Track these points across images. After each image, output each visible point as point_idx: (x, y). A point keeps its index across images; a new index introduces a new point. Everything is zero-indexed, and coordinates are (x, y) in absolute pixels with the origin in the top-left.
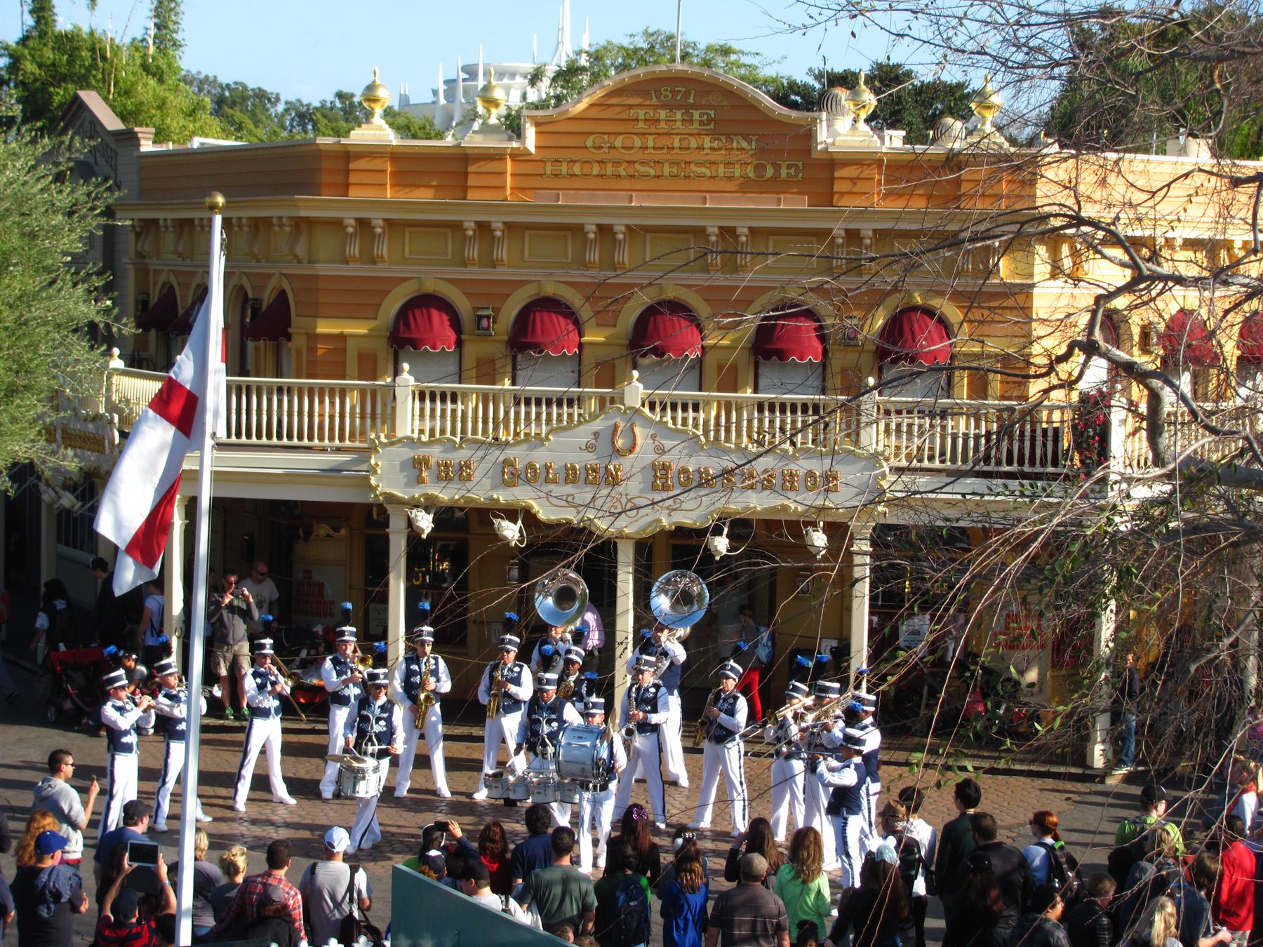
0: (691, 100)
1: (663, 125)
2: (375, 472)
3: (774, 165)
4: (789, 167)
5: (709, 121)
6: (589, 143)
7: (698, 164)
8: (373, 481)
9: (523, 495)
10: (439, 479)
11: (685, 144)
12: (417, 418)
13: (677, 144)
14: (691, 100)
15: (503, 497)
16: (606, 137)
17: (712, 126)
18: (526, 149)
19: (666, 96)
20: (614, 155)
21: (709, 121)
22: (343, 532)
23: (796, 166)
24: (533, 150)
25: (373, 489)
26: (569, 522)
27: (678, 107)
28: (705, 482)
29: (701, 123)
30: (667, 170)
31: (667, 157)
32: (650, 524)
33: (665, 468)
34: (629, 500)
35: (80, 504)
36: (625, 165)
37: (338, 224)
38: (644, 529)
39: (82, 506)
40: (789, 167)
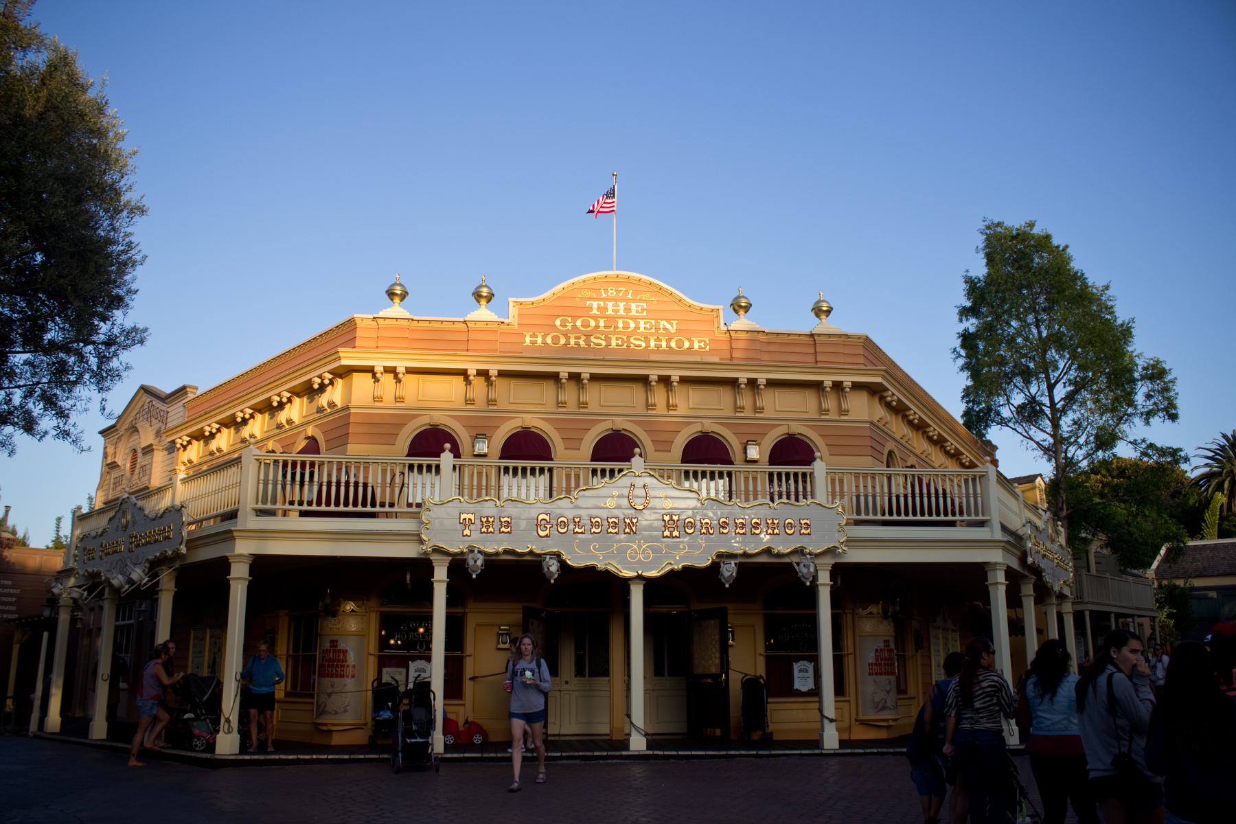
0: (630, 296)
3: (689, 340)
4: (700, 342)
5: (643, 310)
6: (558, 322)
13: (620, 325)
14: (630, 296)
16: (570, 319)
17: (645, 314)
19: (612, 293)
21: (643, 310)
23: (705, 341)
27: (622, 300)
29: (637, 312)
35: (147, 579)
36: (584, 338)
37: (370, 370)
39: (148, 581)
40: (700, 342)
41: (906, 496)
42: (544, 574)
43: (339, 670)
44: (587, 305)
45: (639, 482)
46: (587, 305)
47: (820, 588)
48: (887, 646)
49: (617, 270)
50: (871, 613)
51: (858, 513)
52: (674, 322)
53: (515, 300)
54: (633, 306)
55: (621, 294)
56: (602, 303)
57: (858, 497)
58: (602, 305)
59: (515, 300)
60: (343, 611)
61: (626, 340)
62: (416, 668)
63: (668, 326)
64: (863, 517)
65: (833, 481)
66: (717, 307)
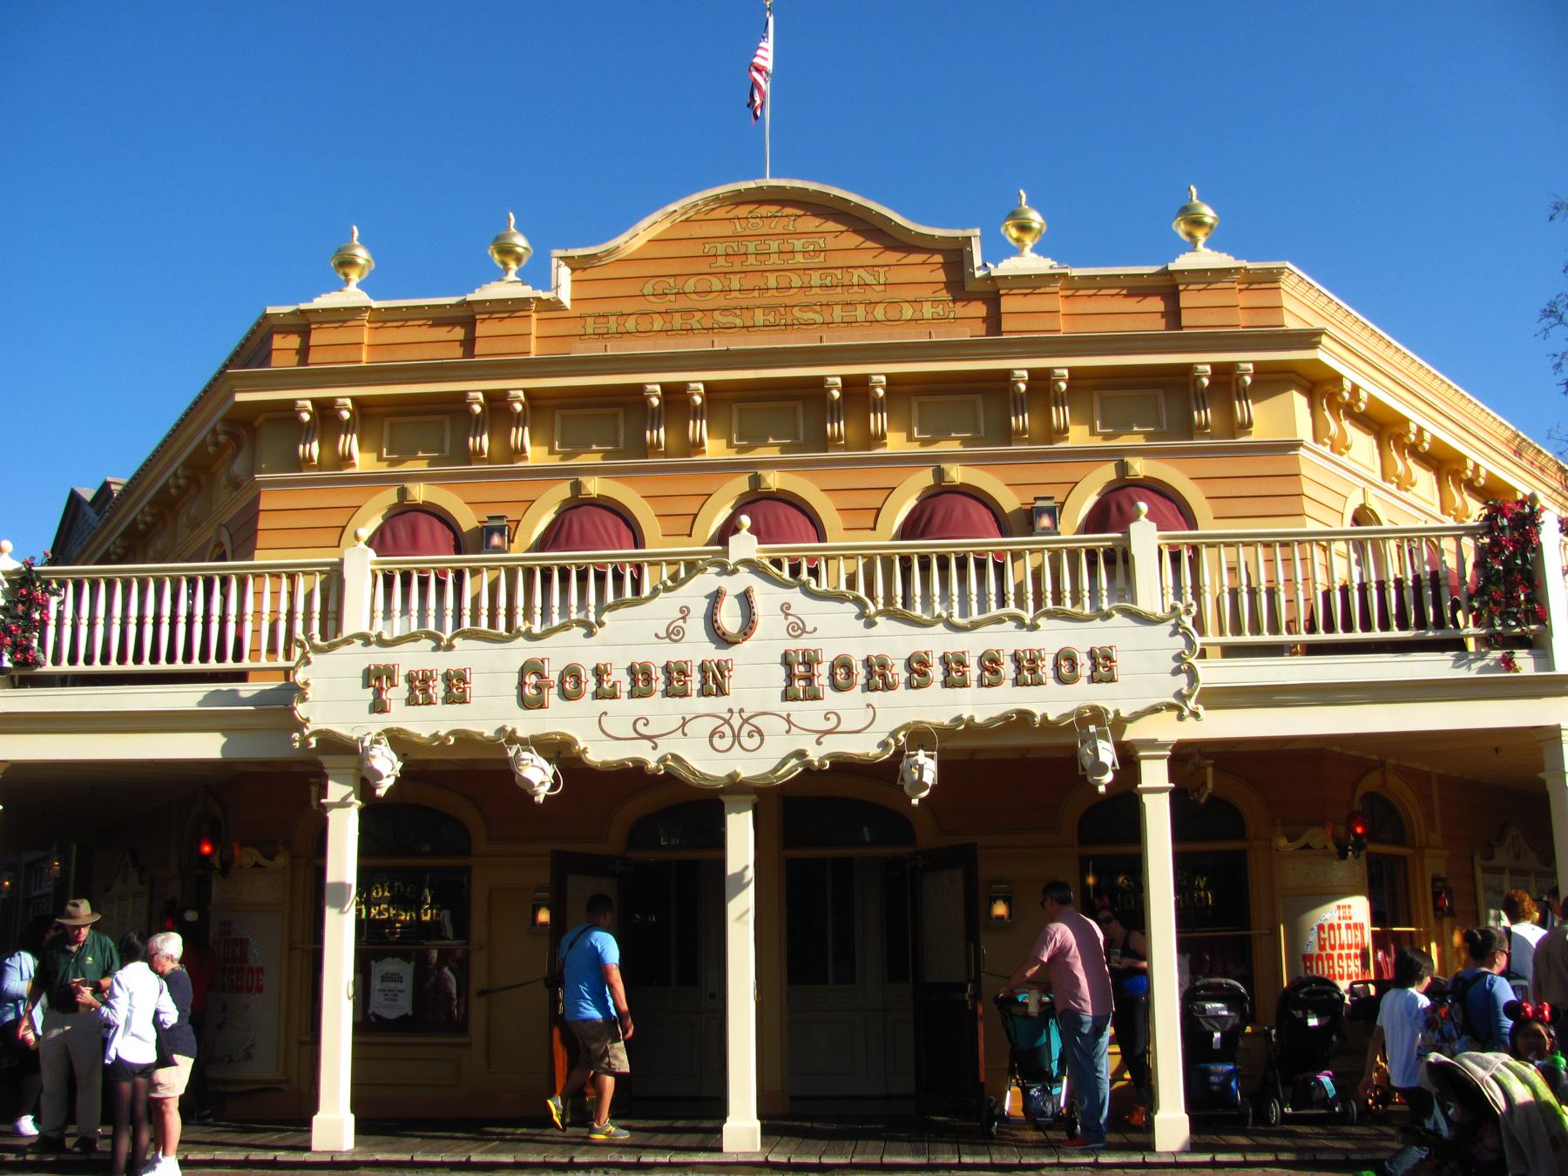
1: (752, 260)
2: (304, 699)
7: (806, 307)
8: (301, 710)
9: (557, 718)
10: (411, 701)
11: (784, 283)
12: (379, 614)
15: (528, 724)
16: (671, 281)
18: (559, 302)
20: (683, 303)
22: (281, 860)
24: (567, 303)
25: (299, 726)
26: (640, 766)
28: (877, 675)
30: (760, 318)
31: (759, 302)
32: (784, 762)
33: (810, 661)
34: (746, 721)
38: (776, 769)
41: (1363, 588)
42: (515, 783)
43: (234, 977)
44: (706, 250)
45: (733, 586)
46: (706, 250)
47: (1147, 799)
48: (1345, 918)
49: (772, 176)
50: (1307, 847)
51: (1237, 630)
52: (882, 271)
53: (562, 253)
54: (798, 244)
55: (773, 225)
56: (735, 245)
57: (1234, 593)
58: (736, 249)
59: (562, 253)
60: (240, 867)
61: (783, 312)
62: (383, 973)
63: (869, 279)
64: (1247, 638)
65: (1176, 558)
66: (968, 233)
